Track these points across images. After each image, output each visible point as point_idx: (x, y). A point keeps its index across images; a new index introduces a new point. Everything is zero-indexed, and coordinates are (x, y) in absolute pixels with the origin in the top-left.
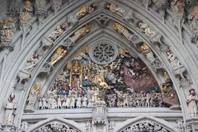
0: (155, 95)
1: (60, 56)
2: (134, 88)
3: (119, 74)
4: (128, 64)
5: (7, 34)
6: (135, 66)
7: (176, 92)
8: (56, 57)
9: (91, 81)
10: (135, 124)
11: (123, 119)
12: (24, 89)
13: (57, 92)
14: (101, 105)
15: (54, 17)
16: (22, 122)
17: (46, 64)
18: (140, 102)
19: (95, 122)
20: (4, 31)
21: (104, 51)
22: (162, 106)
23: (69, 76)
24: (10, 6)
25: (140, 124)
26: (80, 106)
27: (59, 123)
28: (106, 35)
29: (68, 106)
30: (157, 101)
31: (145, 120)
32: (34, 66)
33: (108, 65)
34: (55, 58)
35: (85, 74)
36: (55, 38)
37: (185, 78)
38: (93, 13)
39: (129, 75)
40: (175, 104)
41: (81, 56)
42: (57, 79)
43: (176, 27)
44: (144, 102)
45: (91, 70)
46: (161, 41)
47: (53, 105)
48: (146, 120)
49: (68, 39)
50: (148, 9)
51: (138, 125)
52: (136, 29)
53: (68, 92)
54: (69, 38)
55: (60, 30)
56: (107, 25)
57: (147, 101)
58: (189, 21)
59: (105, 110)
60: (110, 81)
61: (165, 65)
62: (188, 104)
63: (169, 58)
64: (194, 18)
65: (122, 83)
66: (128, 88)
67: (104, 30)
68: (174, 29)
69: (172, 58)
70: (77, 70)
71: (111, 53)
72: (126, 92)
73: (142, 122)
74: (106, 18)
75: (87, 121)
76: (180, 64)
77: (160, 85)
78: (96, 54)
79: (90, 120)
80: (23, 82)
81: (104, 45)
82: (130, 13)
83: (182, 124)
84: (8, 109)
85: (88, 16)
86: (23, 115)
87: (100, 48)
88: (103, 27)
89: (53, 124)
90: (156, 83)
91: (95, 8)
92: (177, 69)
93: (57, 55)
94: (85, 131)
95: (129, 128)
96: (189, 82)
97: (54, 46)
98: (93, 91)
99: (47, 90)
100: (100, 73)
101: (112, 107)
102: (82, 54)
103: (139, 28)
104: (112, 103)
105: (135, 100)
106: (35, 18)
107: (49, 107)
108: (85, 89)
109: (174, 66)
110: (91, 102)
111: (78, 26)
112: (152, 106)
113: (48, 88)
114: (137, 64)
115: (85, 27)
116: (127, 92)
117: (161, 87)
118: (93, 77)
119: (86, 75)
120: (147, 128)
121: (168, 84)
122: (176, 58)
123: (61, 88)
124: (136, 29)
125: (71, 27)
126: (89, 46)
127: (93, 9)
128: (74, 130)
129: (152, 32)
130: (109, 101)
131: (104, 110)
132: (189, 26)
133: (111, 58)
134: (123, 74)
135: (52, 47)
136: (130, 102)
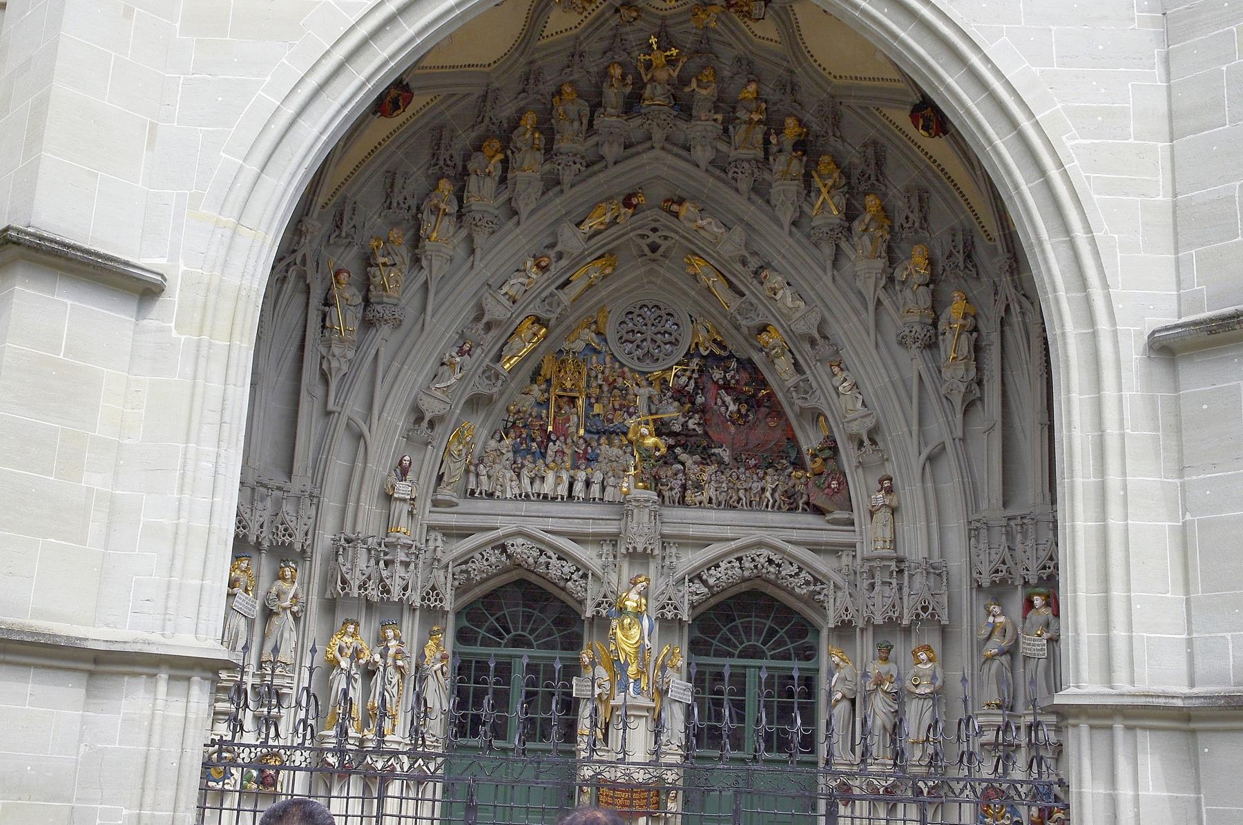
0: (790, 476)
2: (733, 450)
3: (693, 403)
5: (388, 282)
6: (737, 381)
11: (703, 543)
13: (513, 445)
17: (489, 368)
20: (378, 273)
23: (548, 400)
25: (744, 558)
29: (551, 494)
34: (515, 351)
45: (613, 387)
47: (508, 488)
49: (552, 295)
50: (791, 233)
53: (546, 448)
54: (555, 291)
55: (534, 273)
57: (768, 494)
58: (898, 288)
62: (872, 514)
63: (837, 384)
65: (700, 432)
73: (753, 552)
74: (666, 238)
75: (605, 541)
76: (864, 404)
77: (804, 448)
79: (614, 539)
80: (432, 424)
85: (616, 228)
90: (792, 439)
95: (717, 566)
98: (616, 451)
102: (589, 335)
103: (762, 283)
104: (673, 493)
106: (463, 233)
108: (594, 444)
109: (848, 408)
113: (489, 433)
114: (744, 376)
117: (808, 458)
118: (617, 407)
121: (827, 453)
122: (855, 385)
123: (524, 436)
124: (751, 284)
125: (564, 263)
127: (631, 211)
129: (798, 302)
136: (720, 493)
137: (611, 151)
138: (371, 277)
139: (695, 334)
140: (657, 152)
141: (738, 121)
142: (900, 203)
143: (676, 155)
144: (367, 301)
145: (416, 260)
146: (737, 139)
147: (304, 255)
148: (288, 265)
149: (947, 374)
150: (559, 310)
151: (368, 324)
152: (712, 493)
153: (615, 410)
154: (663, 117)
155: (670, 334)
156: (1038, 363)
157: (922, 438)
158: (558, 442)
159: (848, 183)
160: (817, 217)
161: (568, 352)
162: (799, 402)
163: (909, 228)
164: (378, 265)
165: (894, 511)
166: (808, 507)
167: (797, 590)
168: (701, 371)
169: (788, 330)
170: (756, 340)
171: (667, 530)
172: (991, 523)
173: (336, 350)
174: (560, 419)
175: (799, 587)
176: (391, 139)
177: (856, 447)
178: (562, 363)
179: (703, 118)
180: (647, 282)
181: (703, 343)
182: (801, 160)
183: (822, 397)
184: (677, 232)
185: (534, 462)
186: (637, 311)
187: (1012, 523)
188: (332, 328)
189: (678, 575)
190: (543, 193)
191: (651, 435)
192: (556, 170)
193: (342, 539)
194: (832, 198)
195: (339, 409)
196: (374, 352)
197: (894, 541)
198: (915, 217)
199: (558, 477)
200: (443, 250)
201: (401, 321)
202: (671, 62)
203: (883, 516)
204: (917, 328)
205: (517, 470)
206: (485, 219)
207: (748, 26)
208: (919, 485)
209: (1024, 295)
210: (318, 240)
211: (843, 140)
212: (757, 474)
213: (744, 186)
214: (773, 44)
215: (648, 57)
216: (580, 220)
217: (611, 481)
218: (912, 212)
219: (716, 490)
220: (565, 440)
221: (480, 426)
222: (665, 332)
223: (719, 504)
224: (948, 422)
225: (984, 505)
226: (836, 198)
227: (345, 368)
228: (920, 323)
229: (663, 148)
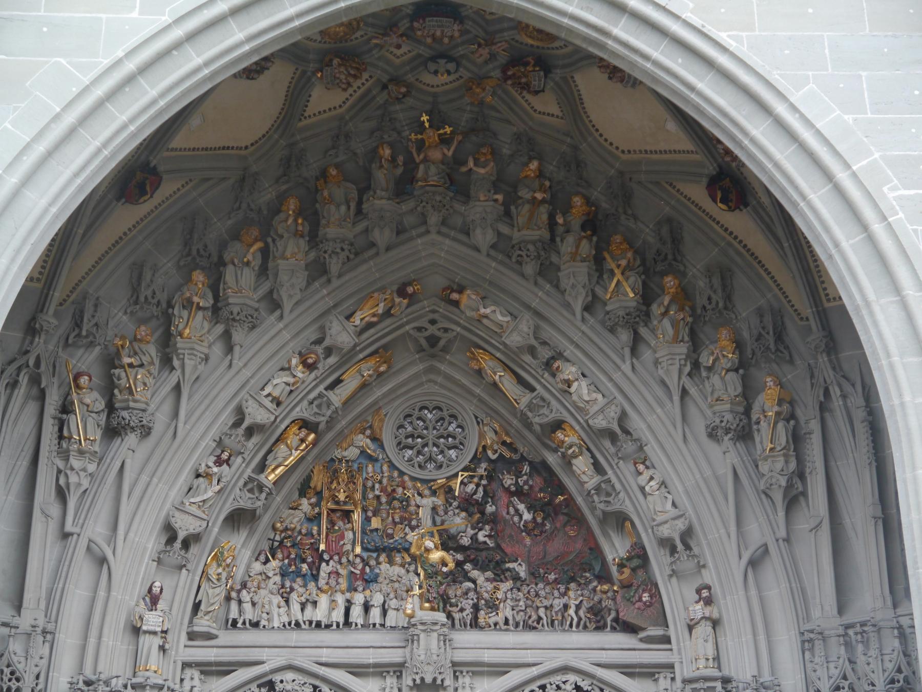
0: (594, 590)
2: (529, 565)
3: (483, 513)
5: (135, 385)
6: (531, 487)
7: (656, 585)
8: (284, 455)
9: (391, 536)
12: (189, 566)
16: (183, 669)
18: (548, 612)
19: (414, 680)
20: (123, 375)
23: (319, 514)
24: (139, 284)
25: (548, 686)
27: (300, 678)
28: (440, 379)
29: (324, 621)
31: (563, 672)
32: (219, 492)
34: (280, 460)
35: (371, 508)
37: (686, 550)
38: (403, 315)
39: (512, 519)
40: (654, 626)
41: (356, 447)
43: (663, 383)
44: (560, 614)
45: (391, 497)
46: (620, 426)
49: (320, 396)
50: (583, 319)
52: (543, 378)
53: (318, 569)
54: (324, 392)
55: (300, 372)
56: (445, 350)
57: (572, 612)
58: (704, 374)
59: (445, 641)
60: (453, 538)
61: (627, 502)
62: (690, 628)
63: (643, 484)
64: (717, 363)
65: (491, 545)
66: (509, 562)
67: (438, 365)
68: (660, 392)
72: (502, 577)
73: (557, 679)
74: (446, 330)
75: (388, 672)
76: (674, 505)
80: (186, 544)
82: (526, 324)
83: (671, 685)
84: (145, 632)
86: (185, 646)
88: (433, 356)
90: (596, 550)
91: (413, 299)
92: (666, 522)
93: (286, 449)
96: (696, 561)
98: (397, 570)
100: (418, 507)
101: (461, 626)
102: (362, 441)
103: (554, 375)
104: (464, 614)
106: (220, 329)
108: (373, 563)
109: (657, 509)
110: (395, 609)
112: (585, 627)
113: (253, 553)
114: (537, 482)
115: (377, 355)
117: (614, 569)
118: (397, 520)
119: (374, 515)
121: (636, 562)
122: (663, 484)
123: (293, 556)
124: (543, 377)
125: (332, 360)
126: (384, 411)
127: (406, 301)
129: (594, 395)
130: (454, 609)
131: (442, 642)
132: (701, 386)
133: (453, 453)
134: (493, 514)
136: (518, 613)
137: (382, 236)
138: (115, 380)
139: (482, 436)
140: (433, 236)
141: (520, 201)
142: (701, 284)
143: (454, 239)
144: (111, 408)
145: (167, 362)
146: (521, 220)
147: (38, 355)
148: (19, 369)
149: (764, 467)
150: (329, 413)
151: (113, 432)
152: (509, 613)
153: (395, 523)
154: (438, 198)
155: (454, 438)
156: (865, 450)
157: (740, 538)
158: (331, 563)
159: (643, 262)
160: (612, 300)
161: (340, 461)
162: (602, 506)
163: (713, 309)
164: (123, 367)
165: (715, 623)
166: (618, 624)
168: (490, 478)
169: (585, 425)
170: (551, 440)
171: (460, 656)
172: (827, 632)
173: (75, 463)
174: (332, 537)
176: (137, 229)
177: (668, 553)
178: (334, 474)
179: (482, 199)
181: (492, 446)
182: (591, 241)
183: (626, 498)
184: (458, 324)
185: (305, 586)
186: (416, 413)
187: (851, 632)
188: (70, 438)
190: (307, 286)
191: (436, 548)
192: (322, 258)
193: (81, 682)
194: (627, 279)
195: (76, 530)
196: (118, 464)
197: (717, 659)
198: (718, 297)
200: (197, 347)
201: (150, 428)
202: (445, 141)
203: (704, 629)
204: (728, 417)
205: (285, 595)
206: (244, 313)
207: (527, 101)
208: (742, 592)
209: (844, 376)
210: (55, 339)
211: (635, 217)
212: (558, 589)
213: (530, 269)
214: (554, 119)
215: (419, 137)
216: (349, 312)
217: (393, 603)
218: (715, 292)
220: (340, 559)
221: (243, 546)
222: (449, 436)
223: (517, 625)
224: (770, 521)
225: (816, 613)
226: (632, 279)
227: (85, 483)
228: (731, 411)
229: (439, 233)
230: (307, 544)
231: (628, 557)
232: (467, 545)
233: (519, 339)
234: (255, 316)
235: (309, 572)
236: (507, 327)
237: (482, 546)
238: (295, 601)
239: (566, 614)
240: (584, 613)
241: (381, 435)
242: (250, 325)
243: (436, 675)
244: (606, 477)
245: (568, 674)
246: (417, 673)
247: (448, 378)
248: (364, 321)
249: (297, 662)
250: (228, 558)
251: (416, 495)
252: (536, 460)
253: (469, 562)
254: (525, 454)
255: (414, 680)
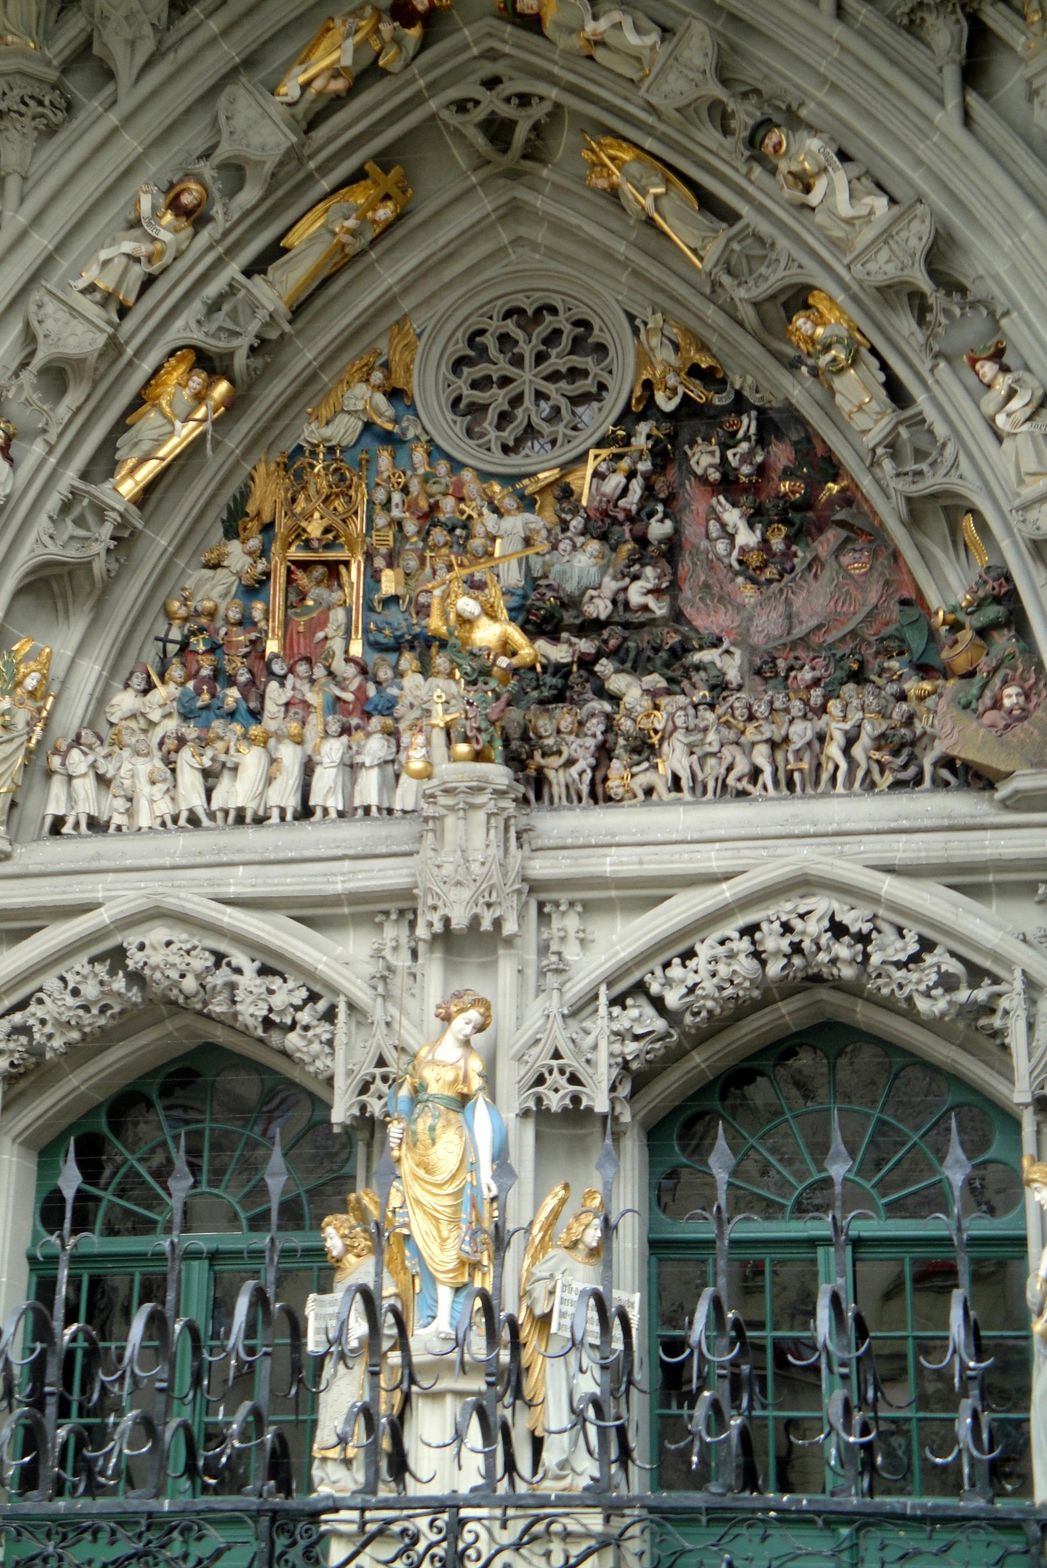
1: (178, 424)
2: (753, 650)
3: (642, 541)
4: (706, 460)
8: (154, 434)
10: (730, 929)
13: (179, 700)
14: (470, 800)
15: (113, 118)
17: (75, 494)
19: (431, 924)
21: (529, 360)
22: (947, 784)
23: (267, 574)
25: (764, 926)
26: (335, 803)
27: (184, 936)
28: (540, 235)
29: (251, 807)
30: (903, 745)
33: (555, 473)
34: (145, 446)
35: (383, 550)
36: (128, 294)
38: (415, 68)
40: (1033, 765)
41: (349, 412)
42: (176, 605)
44: (807, 757)
46: (933, 273)
48: (817, 891)
49: (232, 289)
51: (750, 931)
52: (752, 182)
53: (262, 698)
54: (241, 278)
56: (533, 153)
57: (834, 750)
66: (701, 648)
67: (522, 193)
69: (1015, 404)
70: (326, 522)
71: (585, 373)
72: (685, 684)
73: (785, 908)
74: (524, 100)
75: (387, 913)
78: (466, 391)
81: (530, 312)
87: (505, 340)
88: (513, 175)
89: (142, 947)
93: (161, 421)
94: (365, 986)
95: (689, 954)
97: (130, 351)
99: (107, 686)
100: (493, 539)
103: (773, 171)
104: (574, 771)
105: (743, 740)
107: (118, 819)
108: (385, 673)
111: (309, 179)
112: (870, 786)
113: (113, 669)
114: (781, 454)
116: (696, 677)
119: (390, 565)
120: (819, 949)
121: (993, 612)
123: (206, 672)
124: (747, 176)
125: (249, 196)
127: (414, 33)
128: (291, 984)
129: (868, 200)
130: (555, 761)
135: (114, 362)
139: (644, 358)
158: (290, 680)
167: (922, 1004)
170: (789, 342)
171: (542, 867)
175: (927, 994)
180: (512, 242)
184: (551, 79)
189: (577, 987)
199: (273, 761)
219: (692, 753)
221: (80, 650)
230: (239, 644)
231: (970, 604)
232: (603, 617)
233: (682, 85)
234: (47, 102)
235: (243, 705)
236: (652, 62)
237: (640, 617)
238: (187, 768)
239: (823, 759)
240: (866, 751)
241: (408, 383)
242: (40, 123)
243: (478, 910)
244: (911, 412)
245: (814, 895)
246: (435, 908)
247: (559, 228)
248: (312, 91)
249: (174, 901)
250: (25, 676)
251: (485, 511)
252: (775, 404)
253: (609, 656)
254: (746, 393)
255: (431, 924)
